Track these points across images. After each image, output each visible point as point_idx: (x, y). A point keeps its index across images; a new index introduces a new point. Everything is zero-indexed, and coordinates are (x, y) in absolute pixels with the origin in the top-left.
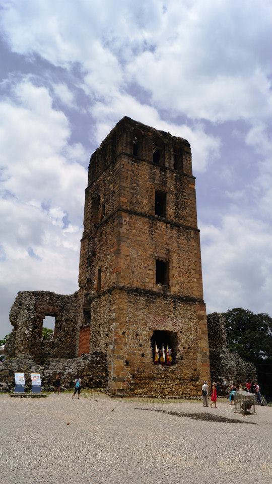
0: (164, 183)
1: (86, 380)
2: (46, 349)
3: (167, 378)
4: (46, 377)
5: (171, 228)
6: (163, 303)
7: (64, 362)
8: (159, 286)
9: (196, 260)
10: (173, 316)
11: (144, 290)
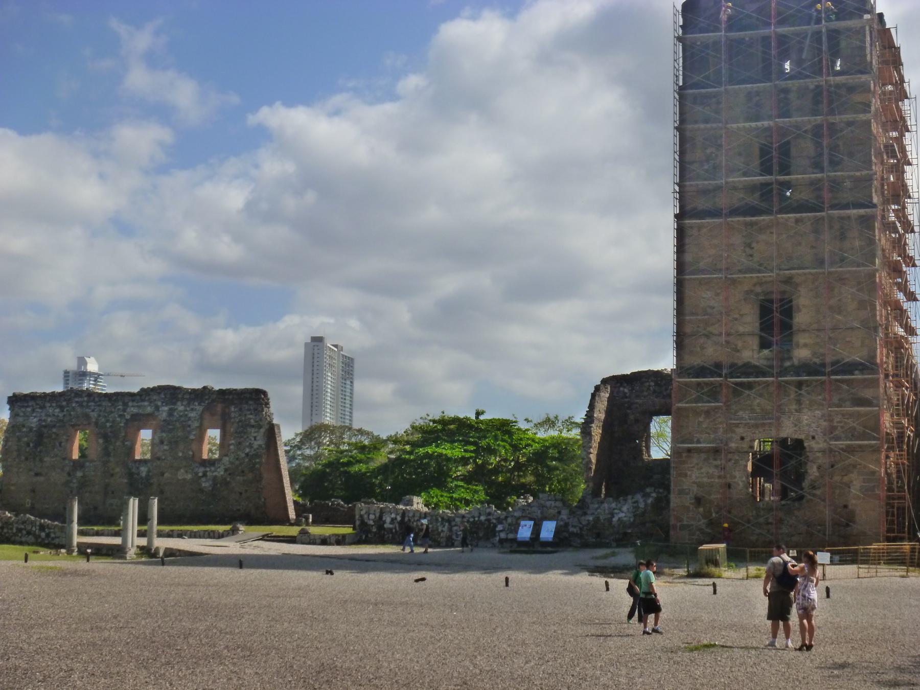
2: (656, 477)
4: (584, 526)
7: (610, 505)
8: (766, 352)
10: (794, 407)
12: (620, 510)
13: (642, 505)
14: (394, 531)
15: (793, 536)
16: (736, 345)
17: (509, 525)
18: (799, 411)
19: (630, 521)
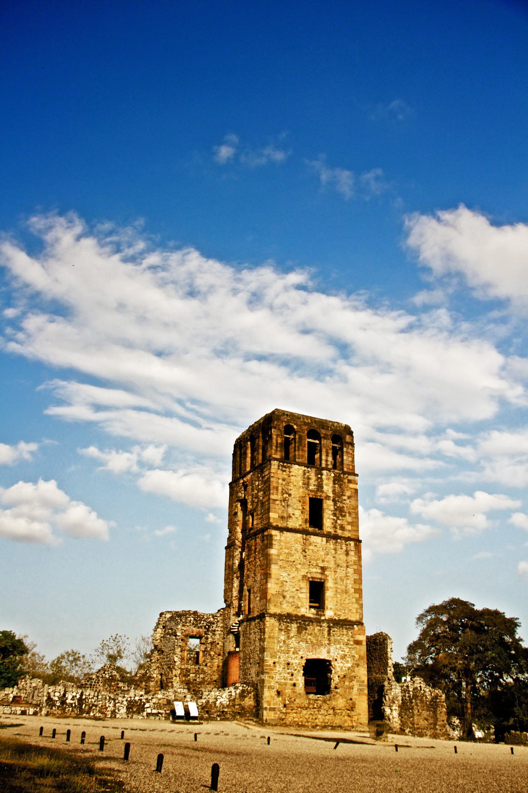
0: (320, 487)
1: (237, 709)
2: (191, 675)
3: (319, 708)
4: (200, 706)
5: (327, 542)
7: (215, 693)
8: (313, 610)
9: (356, 577)
10: (327, 642)
11: (296, 616)
13: (233, 694)
14: (74, 705)
15: (326, 715)
17: (154, 704)
18: (329, 644)
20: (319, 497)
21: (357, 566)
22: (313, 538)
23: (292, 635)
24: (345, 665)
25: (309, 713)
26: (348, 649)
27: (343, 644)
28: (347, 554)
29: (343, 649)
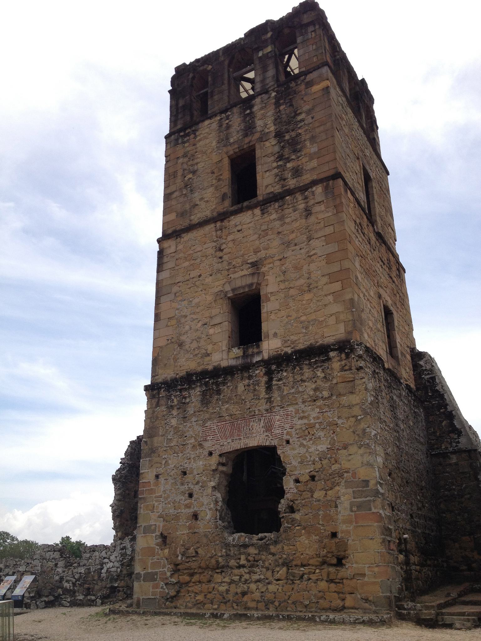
0: (249, 129)
3: (252, 566)
5: (263, 214)
6: (241, 387)
12: (109, 559)
15: (269, 583)
16: (206, 350)
19: (117, 571)
20: (245, 147)
21: (331, 228)
22: (235, 220)
23: (191, 410)
24: (310, 450)
25: (227, 579)
26: (318, 410)
27: (304, 402)
28: (308, 212)
29: (303, 411)
